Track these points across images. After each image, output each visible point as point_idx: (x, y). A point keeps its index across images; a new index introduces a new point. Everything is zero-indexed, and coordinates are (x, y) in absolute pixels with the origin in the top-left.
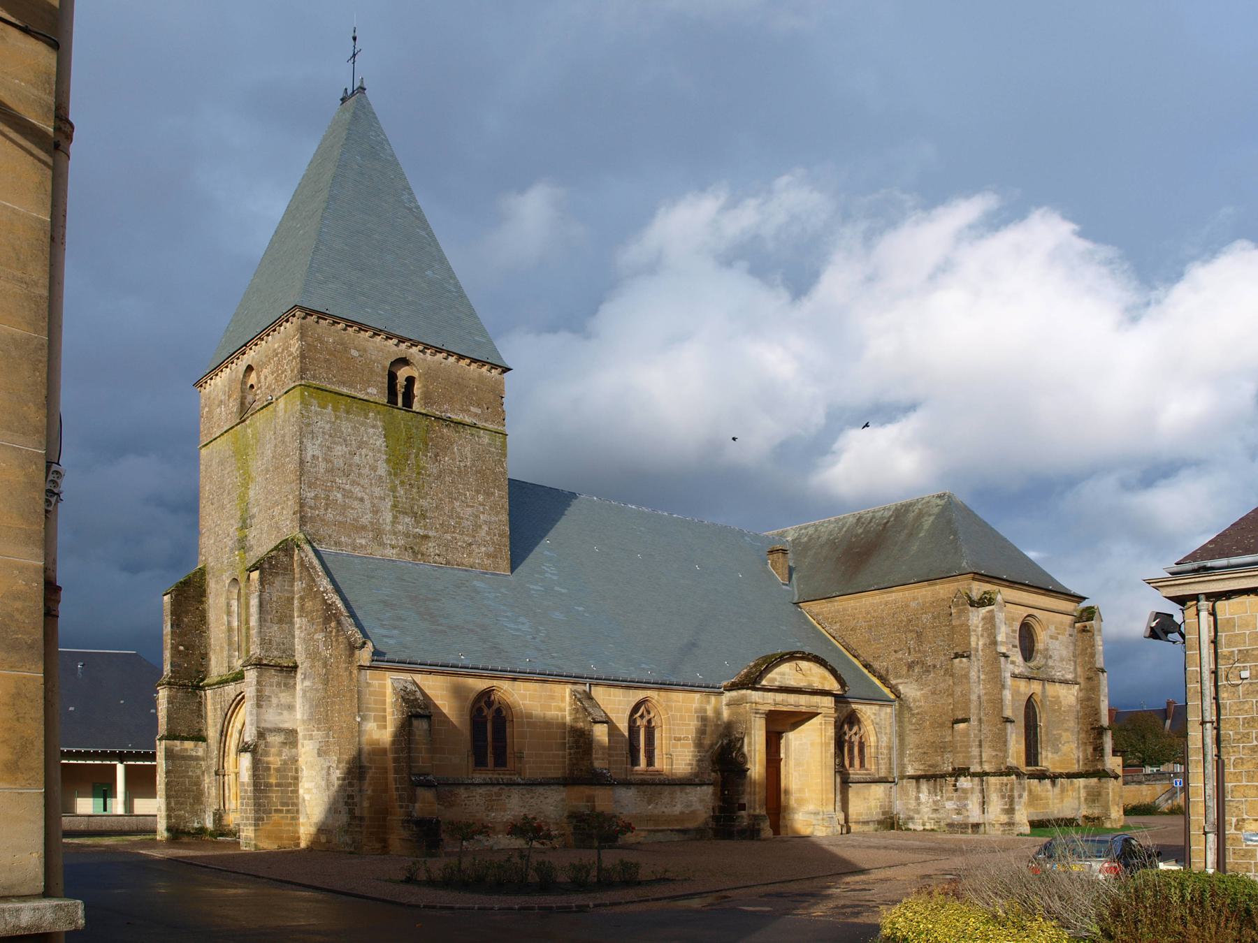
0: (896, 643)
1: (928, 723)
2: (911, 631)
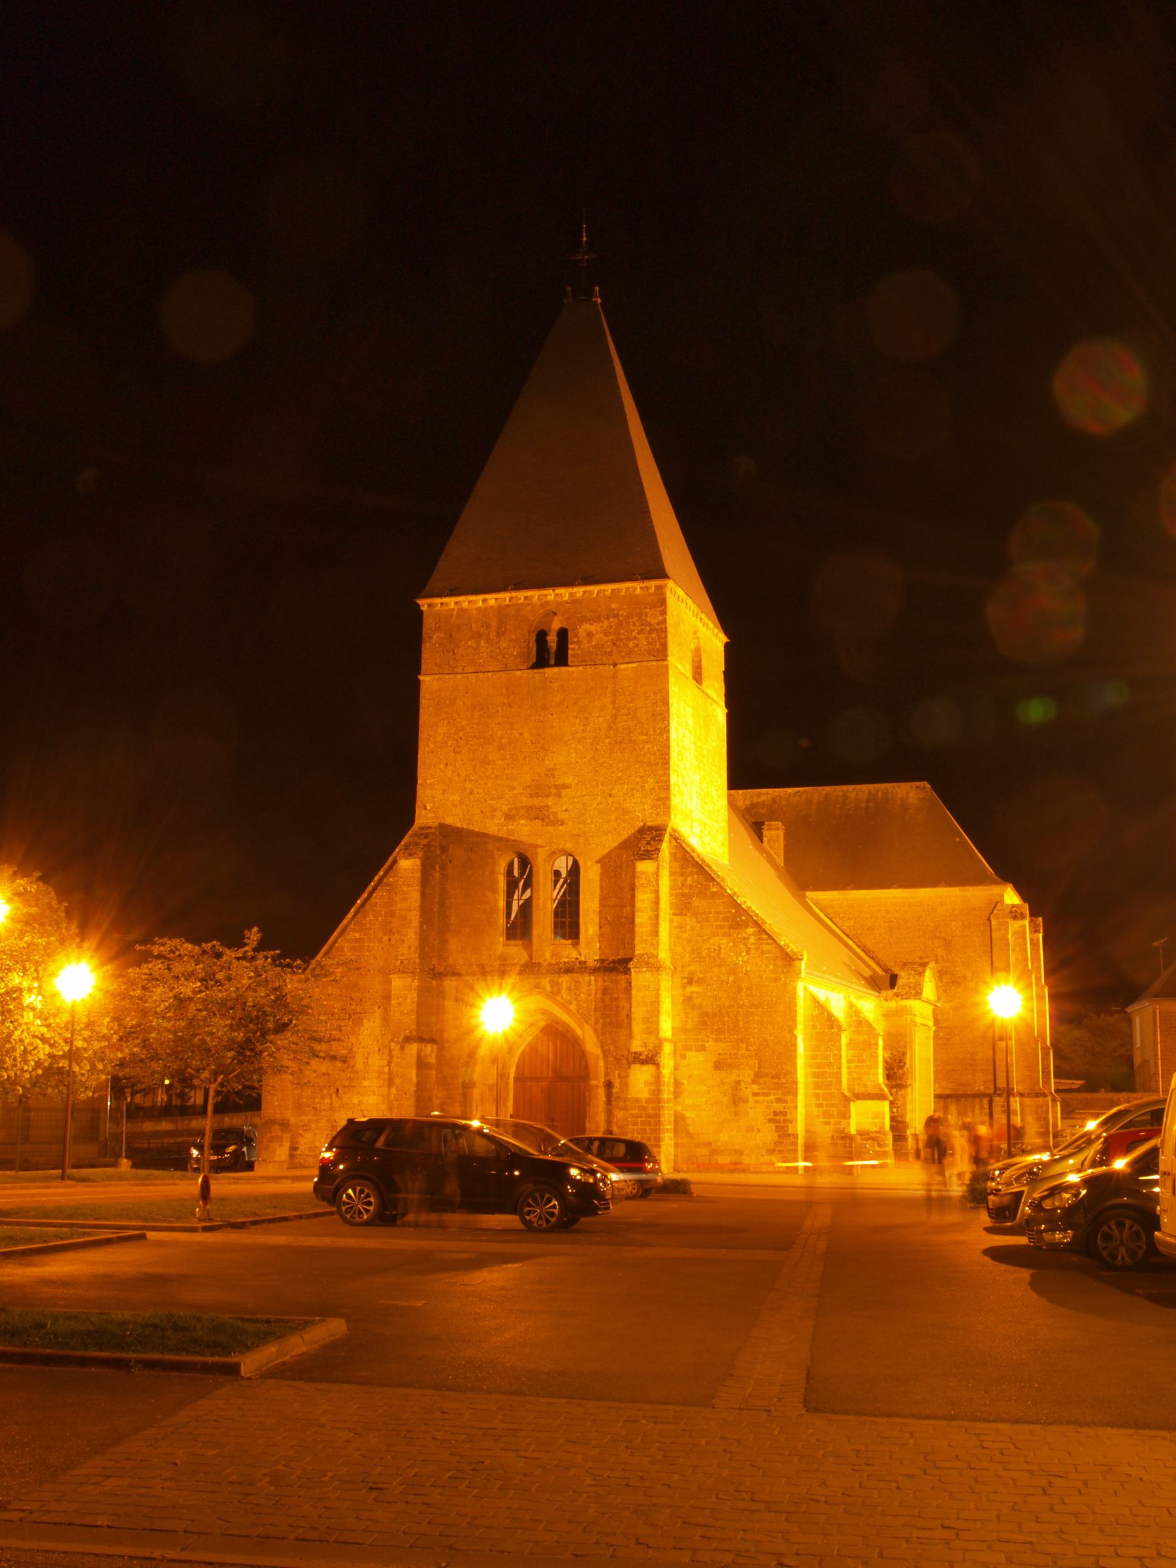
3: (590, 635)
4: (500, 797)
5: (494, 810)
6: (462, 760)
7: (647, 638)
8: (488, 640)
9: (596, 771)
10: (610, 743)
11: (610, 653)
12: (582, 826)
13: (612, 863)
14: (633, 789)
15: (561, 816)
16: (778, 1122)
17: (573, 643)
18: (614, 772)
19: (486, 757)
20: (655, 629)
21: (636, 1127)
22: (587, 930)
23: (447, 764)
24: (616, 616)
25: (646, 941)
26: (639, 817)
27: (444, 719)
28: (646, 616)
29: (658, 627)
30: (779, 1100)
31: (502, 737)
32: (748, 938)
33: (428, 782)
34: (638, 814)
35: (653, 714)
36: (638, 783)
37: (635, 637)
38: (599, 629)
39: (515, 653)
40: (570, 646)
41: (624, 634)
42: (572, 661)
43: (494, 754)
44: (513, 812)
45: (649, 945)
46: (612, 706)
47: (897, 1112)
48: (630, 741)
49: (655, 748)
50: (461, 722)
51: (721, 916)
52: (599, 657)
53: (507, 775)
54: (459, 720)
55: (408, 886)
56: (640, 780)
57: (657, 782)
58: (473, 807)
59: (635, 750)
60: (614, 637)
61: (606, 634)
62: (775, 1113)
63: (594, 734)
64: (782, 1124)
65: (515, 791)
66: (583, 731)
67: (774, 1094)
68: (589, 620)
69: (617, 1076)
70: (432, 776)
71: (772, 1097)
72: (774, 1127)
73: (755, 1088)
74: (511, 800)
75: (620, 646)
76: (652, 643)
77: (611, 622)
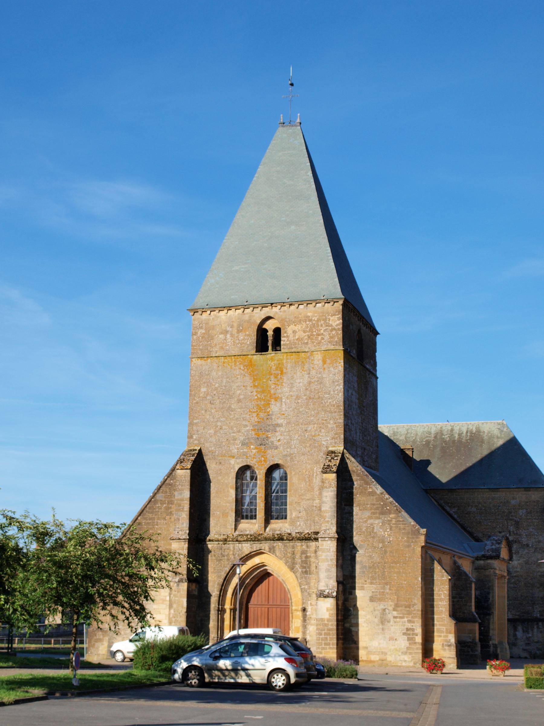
0: (500, 527)
1: (523, 583)
2: (511, 520)
3: (294, 332)
4: (239, 432)
6: (215, 408)
7: (329, 334)
8: (232, 335)
10: (306, 399)
11: (307, 343)
12: (289, 450)
13: (307, 473)
14: (320, 427)
16: (409, 635)
17: (284, 337)
18: (308, 417)
19: (230, 407)
20: (335, 329)
21: (321, 637)
22: (291, 514)
23: (206, 411)
24: (310, 320)
25: (328, 522)
26: (324, 445)
27: (204, 383)
28: (329, 320)
29: (336, 328)
30: (409, 621)
31: (240, 395)
32: (391, 521)
33: (195, 421)
34: (323, 443)
35: (333, 381)
36: (323, 424)
37: (322, 334)
38: (300, 328)
39: (248, 343)
40: (282, 339)
41: (315, 332)
42: (284, 348)
44: (247, 441)
45: (330, 524)
46: (308, 376)
47: (484, 629)
48: (319, 397)
49: (334, 402)
50: (215, 385)
51: (375, 507)
52: (300, 346)
53: (243, 418)
54: (214, 384)
55: (182, 486)
56: (325, 422)
57: (335, 423)
58: (222, 437)
59: (322, 403)
60: (309, 334)
61: (304, 332)
62: (408, 629)
63: (297, 393)
64: (411, 636)
65: (248, 428)
66: (290, 391)
67: (407, 617)
69: (309, 605)
71: (406, 619)
72: (406, 638)
73: (395, 613)
74: (246, 433)
75: (313, 339)
77: (307, 325)
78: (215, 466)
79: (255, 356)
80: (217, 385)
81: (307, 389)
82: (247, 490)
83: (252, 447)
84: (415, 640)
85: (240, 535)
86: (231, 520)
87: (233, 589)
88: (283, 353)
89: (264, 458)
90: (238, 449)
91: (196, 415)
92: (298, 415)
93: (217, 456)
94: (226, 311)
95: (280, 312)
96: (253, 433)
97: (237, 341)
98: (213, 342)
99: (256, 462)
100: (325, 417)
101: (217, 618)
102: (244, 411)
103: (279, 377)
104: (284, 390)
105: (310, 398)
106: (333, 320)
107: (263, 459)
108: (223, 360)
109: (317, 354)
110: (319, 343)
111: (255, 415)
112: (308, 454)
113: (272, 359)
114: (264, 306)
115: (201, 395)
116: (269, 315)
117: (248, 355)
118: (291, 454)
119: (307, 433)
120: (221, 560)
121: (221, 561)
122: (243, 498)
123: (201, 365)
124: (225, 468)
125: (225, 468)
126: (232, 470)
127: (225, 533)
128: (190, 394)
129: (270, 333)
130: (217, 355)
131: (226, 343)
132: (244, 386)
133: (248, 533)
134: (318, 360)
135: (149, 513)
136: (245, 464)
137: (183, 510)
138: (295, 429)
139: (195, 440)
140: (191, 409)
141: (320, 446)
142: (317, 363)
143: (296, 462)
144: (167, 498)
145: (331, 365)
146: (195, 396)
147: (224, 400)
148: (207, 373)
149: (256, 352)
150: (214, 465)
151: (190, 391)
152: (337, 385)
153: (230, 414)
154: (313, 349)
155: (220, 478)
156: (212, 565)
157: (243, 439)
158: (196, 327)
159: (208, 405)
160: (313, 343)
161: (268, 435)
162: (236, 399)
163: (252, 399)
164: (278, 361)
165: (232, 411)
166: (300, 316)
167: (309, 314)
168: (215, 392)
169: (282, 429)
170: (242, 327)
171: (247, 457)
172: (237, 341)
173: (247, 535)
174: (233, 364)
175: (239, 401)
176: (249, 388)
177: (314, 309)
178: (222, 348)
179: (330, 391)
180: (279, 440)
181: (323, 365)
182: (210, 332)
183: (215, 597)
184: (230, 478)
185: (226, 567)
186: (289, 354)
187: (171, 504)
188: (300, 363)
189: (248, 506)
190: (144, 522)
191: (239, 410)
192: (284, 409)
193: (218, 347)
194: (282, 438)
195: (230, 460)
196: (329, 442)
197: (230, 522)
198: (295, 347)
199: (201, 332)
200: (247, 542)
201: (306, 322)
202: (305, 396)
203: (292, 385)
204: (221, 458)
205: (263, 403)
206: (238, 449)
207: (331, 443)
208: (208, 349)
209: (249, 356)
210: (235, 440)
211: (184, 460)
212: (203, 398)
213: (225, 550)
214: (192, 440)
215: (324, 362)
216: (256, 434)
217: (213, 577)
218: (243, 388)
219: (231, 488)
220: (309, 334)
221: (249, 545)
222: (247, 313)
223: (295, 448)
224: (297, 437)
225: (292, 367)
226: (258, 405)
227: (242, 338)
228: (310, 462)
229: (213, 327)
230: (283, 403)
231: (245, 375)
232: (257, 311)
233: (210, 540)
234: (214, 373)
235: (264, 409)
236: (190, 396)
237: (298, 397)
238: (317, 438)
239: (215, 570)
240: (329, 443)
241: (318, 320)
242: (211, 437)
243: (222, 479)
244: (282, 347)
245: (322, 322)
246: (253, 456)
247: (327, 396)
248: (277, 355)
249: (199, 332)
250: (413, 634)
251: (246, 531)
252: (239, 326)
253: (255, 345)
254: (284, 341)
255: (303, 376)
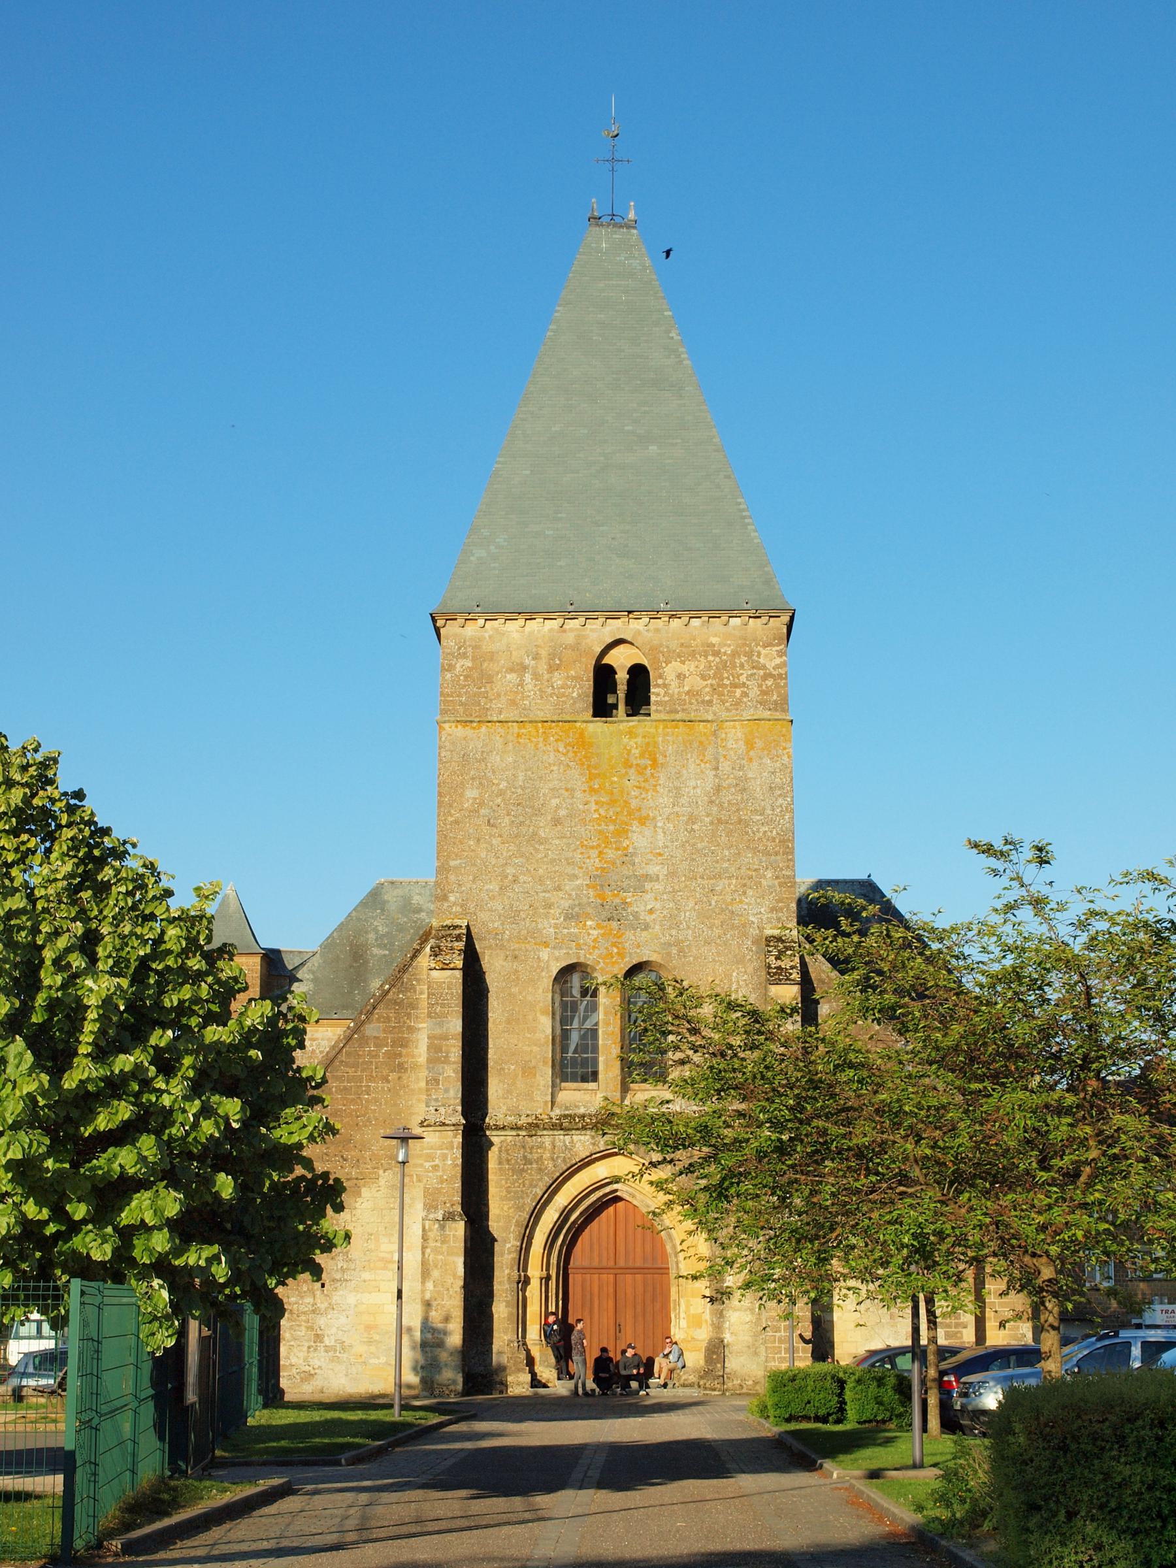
3: (681, 677)
4: (558, 888)
5: (549, 906)
6: (500, 836)
7: (760, 686)
8: (536, 676)
9: (694, 860)
10: (712, 823)
11: (710, 702)
12: (674, 932)
14: (745, 885)
15: (644, 916)
17: (658, 686)
18: (717, 862)
19: (535, 834)
20: (771, 675)
24: (716, 654)
26: (753, 923)
27: (473, 779)
31: (558, 807)
33: (452, 863)
34: (751, 918)
35: (771, 787)
36: (751, 877)
37: (744, 684)
39: (575, 695)
40: (652, 690)
41: (728, 678)
42: (657, 711)
43: (547, 830)
44: (577, 909)
46: (714, 773)
48: (740, 821)
49: (774, 832)
50: (498, 785)
53: (567, 859)
54: (496, 781)
55: (443, 1006)
57: (777, 878)
59: (747, 833)
60: (714, 682)
61: (703, 677)
65: (578, 882)
68: (679, 656)
70: (456, 855)
74: (574, 893)
75: (723, 695)
76: (764, 693)
77: (710, 662)
78: (504, 963)
79: (591, 726)
80: (503, 785)
81: (712, 802)
82: (573, 1018)
83: (589, 923)
84: (962, 1338)
85: (566, 1116)
86: (542, 1083)
87: (546, 1235)
88: (656, 721)
89: (618, 948)
90: (556, 926)
91: (456, 850)
92: (694, 857)
93: (508, 941)
94: (521, 622)
95: (647, 631)
96: (592, 893)
97: (549, 690)
98: (493, 690)
99: (600, 956)
100: (754, 864)
101: (516, 1298)
102: (569, 845)
103: (648, 772)
104: (661, 801)
105: (720, 821)
106: (766, 656)
107: (615, 950)
108: (516, 730)
109: (734, 727)
110: (737, 704)
111: (594, 853)
112: (718, 941)
113: (631, 734)
114: (612, 614)
115: (466, 806)
116: (622, 637)
117: (575, 722)
118: (678, 943)
119: (715, 898)
120: (523, 1170)
121: (524, 1174)
122: (565, 1035)
123: (465, 738)
124: (528, 967)
125: (528, 967)
126: (544, 974)
127: (529, 1112)
128: (440, 804)
129: (622, 677)
130: (502, 717)
131: (523, 693)
132: (567, 790)
133: (582, 1111)
134: (737, 741)
135: (347, 1065)
136: (575, 961)
137: (446, 1061)
138: (686, 886)
139: (455, 904)
140: (443, 836)
141: (744, 926)
142: (734, 746)
143: (691, 959)
144: (390, 1032)
145: (766, 752)
146: (451, 806)
147: (521, 819)
148: (478, 756)
149: (595, 715)
150: (501, 962)
151: (440, 794)
152: (780, 795)
153: (537, 850)
154: (724, 715)
155: (515, 990)
156: (503, 1182)
157: (567, 905)
158: (452, 654)
159: (483, 827)
160: (723, 702)
161: (626, 898)
162: (549, 818)
163: (588, 819)
164: (644, 737)
165: (542, 844)
166: (693, 643)
167: (714, 640)
168: (499, 800)
169: (658, 886)
170: (560, 660)
171: (578, 944)
172: (549, 690)
173: (583, 1116)
174: (541, 739)
175: (557, 822)
176: (578, 794)
177: (722, 629)
178: (513, 703)
179: (764, 809)
180: (651, 911)
181: (748, 752)
182: (485, 665)
183: (510, 1253)
184: (541, 991)
185: (535, 1186)
186: (669, 724)
187: (401, 1046)
188: (695, 745)
189: (575, 1051)
190: (336, 1087)
191: (557, 842)
192: (661, 844)
193: (503, 699)
194: (658, 905)
195: (539, 951)
196: (764, 918)
197: (542, 1088)
198: (683, 710)
199: (462, 665)
200: (583, 1132)
201: (706, 657)
202: (708, 816)
203: (677, 793)
204: (517, 946)
205: (611, 828)
206: (556, 926)
207: (769, 921)
208: (479, 704)
209: (578, 724)
210: (550, 908)
211: (441, 950)
212: (470, 811)
213: (532, 1148)
214: (446, 905)
215: (750, 745)
216: (599, 896)
217: (505, 1208)
218: (566, 794)
219: (543, 1013)
220: (714, 682)
221: (588, 1137)
222: (571, 630)
223: (688, 927)
224: (691, 904)
225: (677, 752)
226: (600, 832)
227: (559, 682)
228: (722, 959)
229: (492, 657)
230: (660, 831)
231: (568, 765)
232: (594, 627)
233: (497, 1128)
234: (495, 759)
235: (616, 842)
236: (439, 807)
237: (692, 819)
238: (734, 908)
239: (509, 1192)
240: (765, 921)
241: (735, 654)
242: (493, 898)
243: (520, 993)
244: (653, 708)
245: (743, 659)
246: (592, 944)
247: (758, 818)
248: (643, 724)
249: (458, 666)
250: (957, 1325)
251: (578, 1107)
252: (552, 656)
253: (591, 699)
254: (656, 694)
255: (702, 772)
